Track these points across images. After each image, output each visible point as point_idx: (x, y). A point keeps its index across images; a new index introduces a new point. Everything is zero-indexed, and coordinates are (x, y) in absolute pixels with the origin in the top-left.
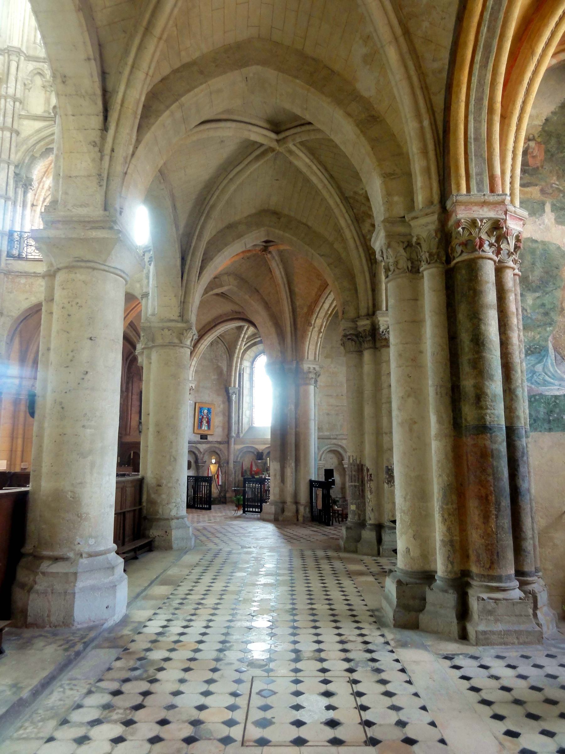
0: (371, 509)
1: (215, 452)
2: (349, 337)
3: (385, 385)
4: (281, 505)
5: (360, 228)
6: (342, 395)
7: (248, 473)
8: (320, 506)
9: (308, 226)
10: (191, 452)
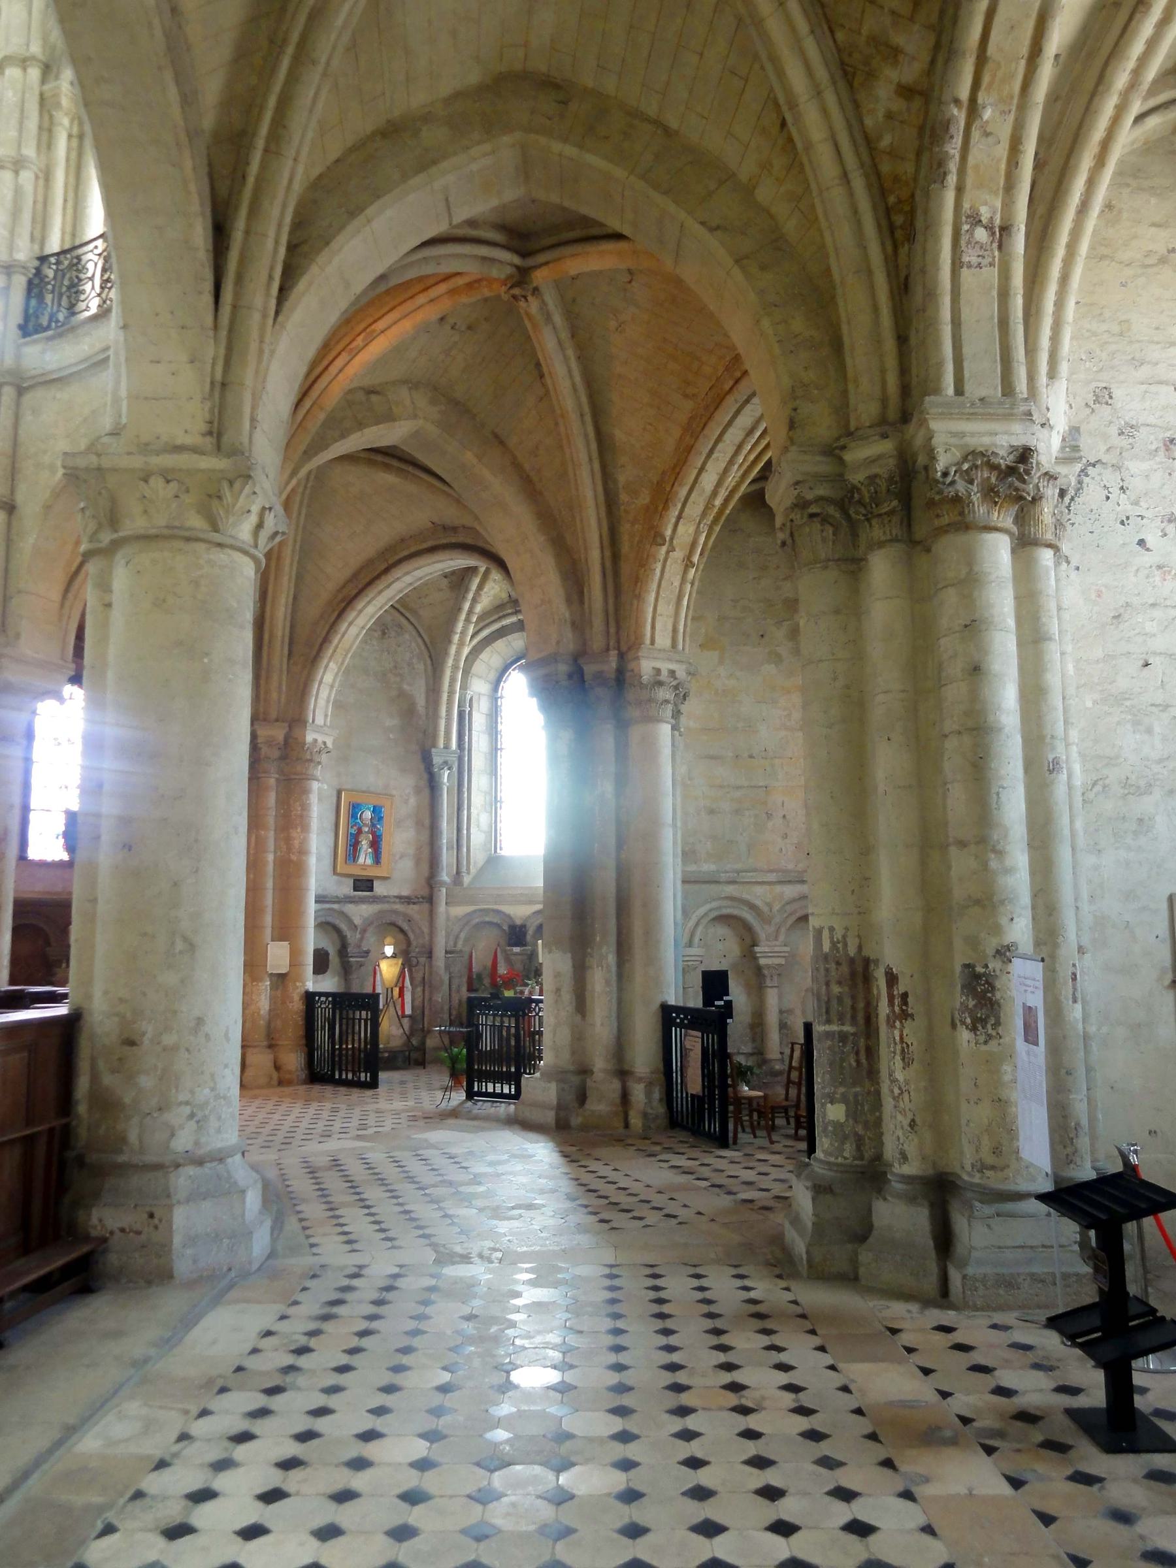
0: (906, 1123)
1: (393, 924)
2: (814, 509)
3: (955, 669)
4: (575, 1080)
5: (857, 105)
6: (751, 757)
7: (487, 981)
8: (695, 1084)
9: (667, 131)
10: (325, 926)
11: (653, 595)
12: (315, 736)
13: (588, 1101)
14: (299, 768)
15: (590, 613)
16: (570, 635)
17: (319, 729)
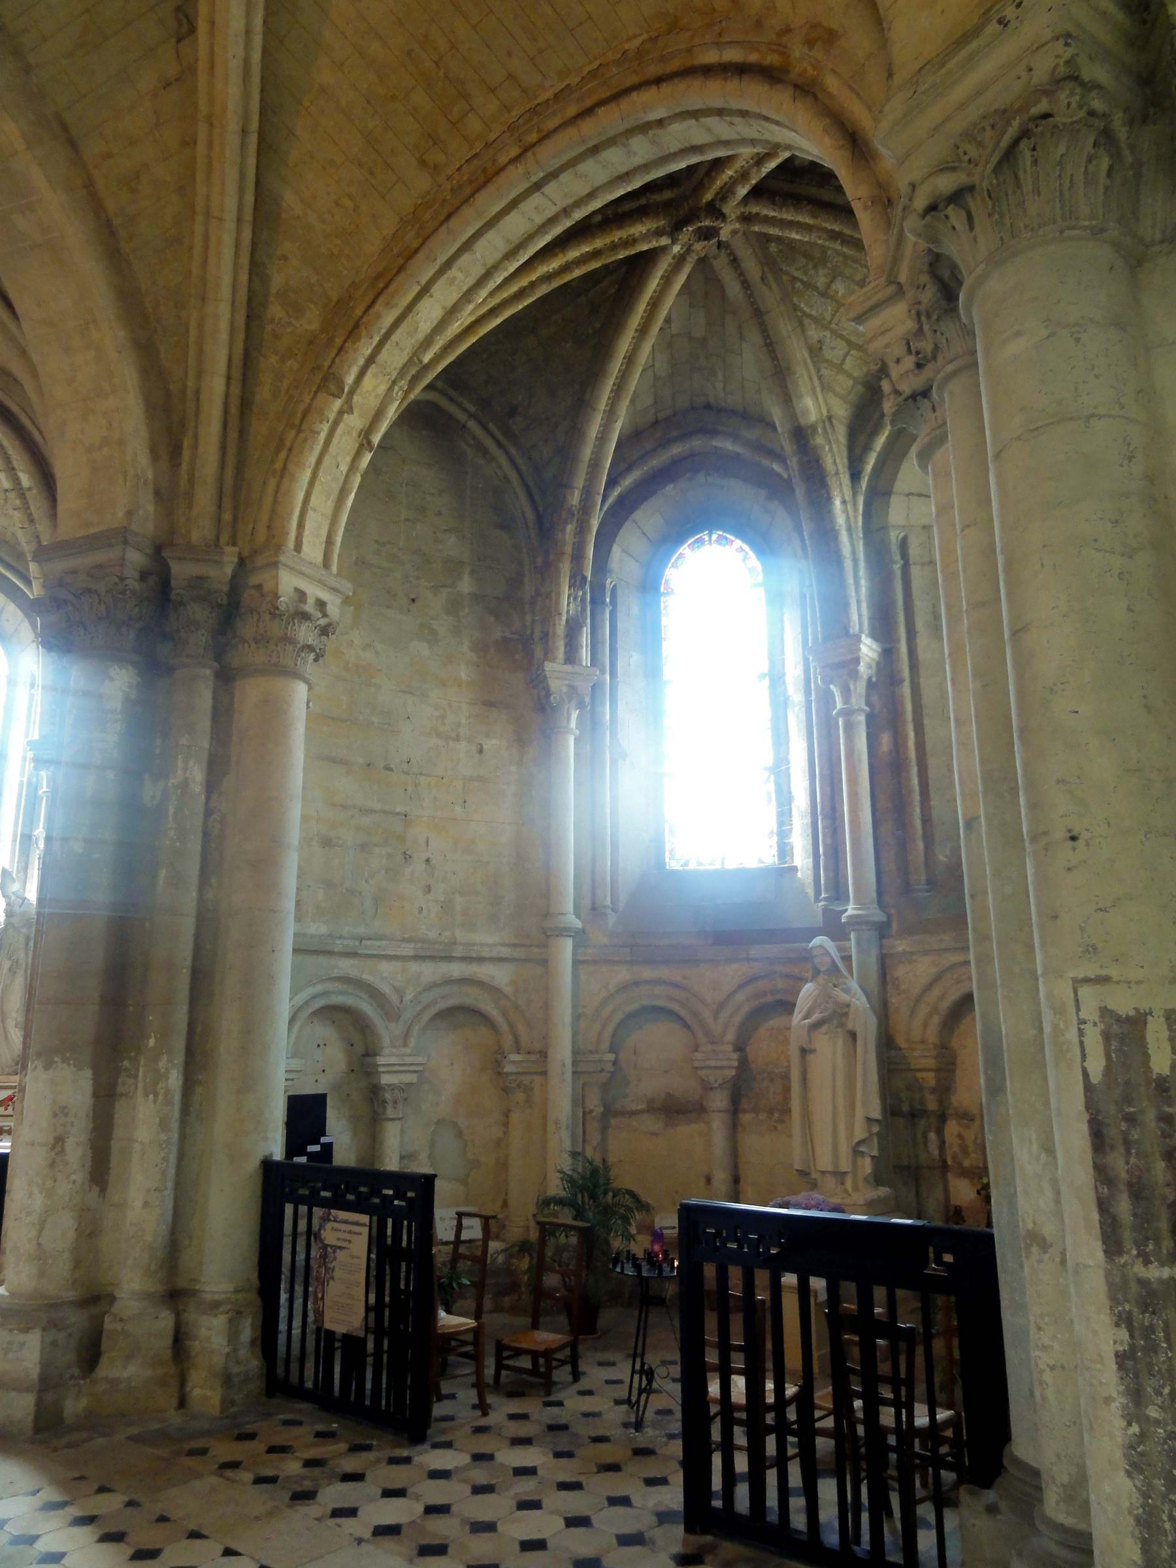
4: (77, 1319)
6: (388, 768)
11: (308, 474)
13: (104, 1360)
15: (191, 481)
16: (151, 508)
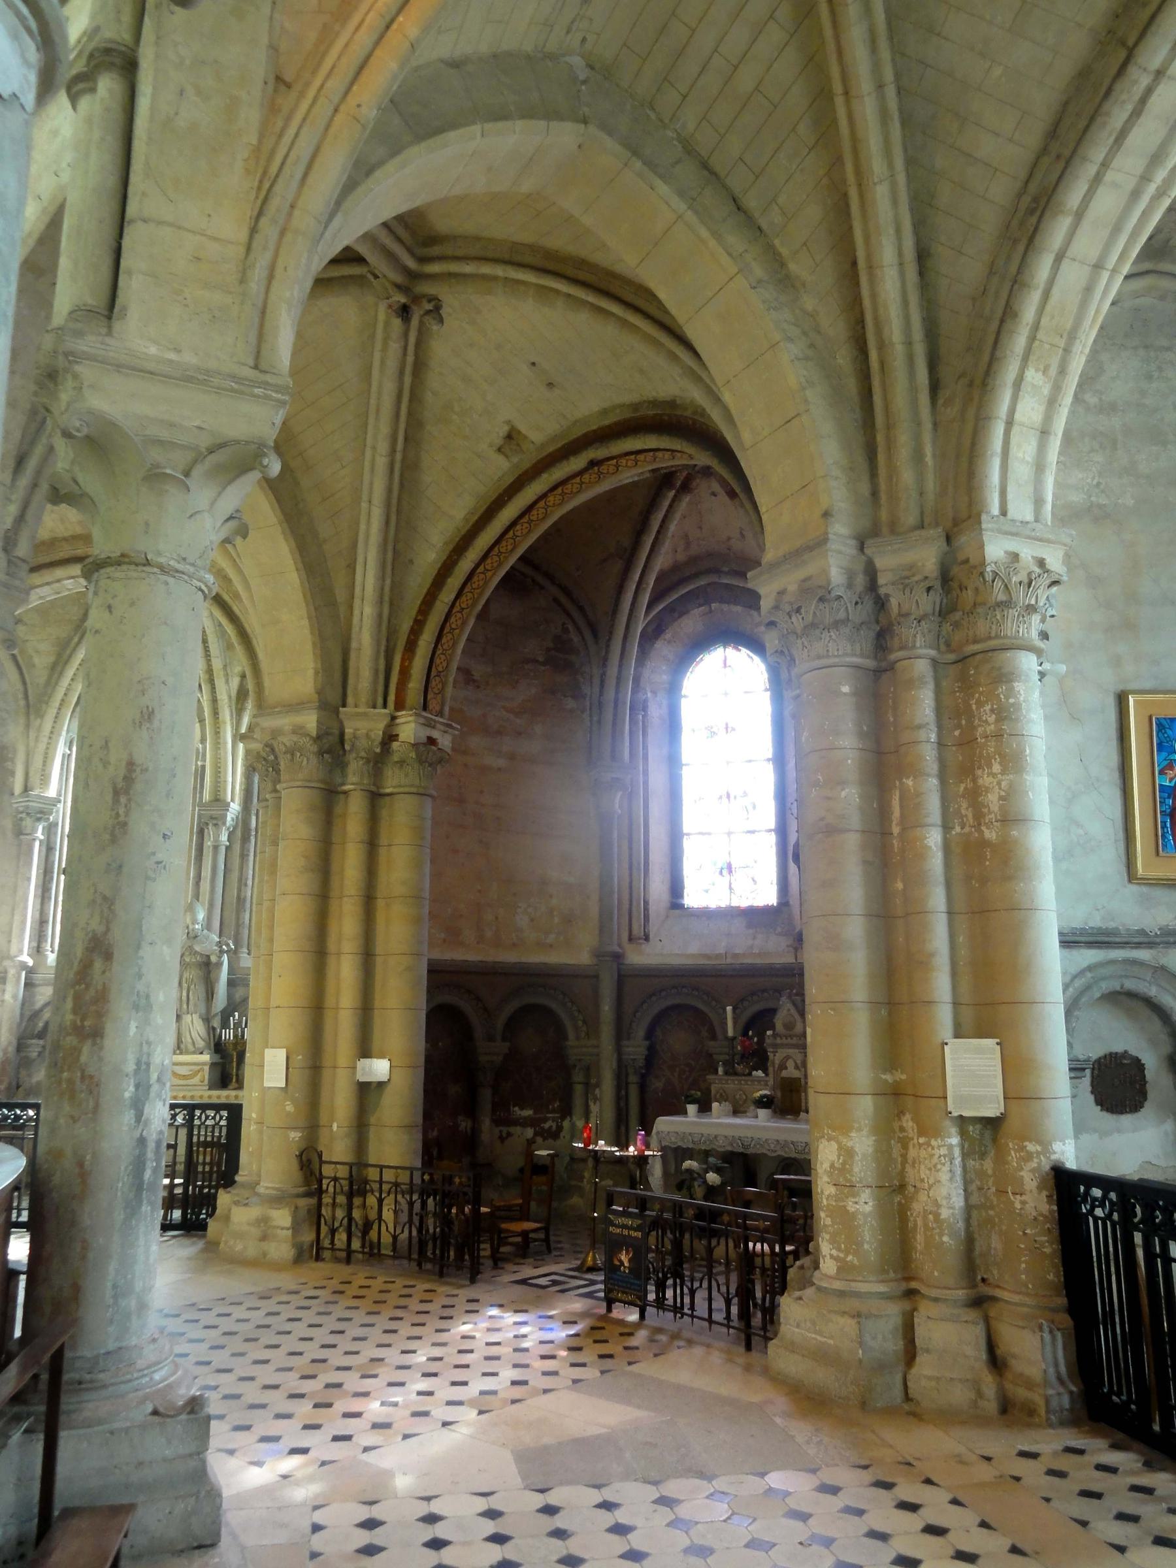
12: (1012, 545)
14: (982, 627)
17: (1017, 531)
